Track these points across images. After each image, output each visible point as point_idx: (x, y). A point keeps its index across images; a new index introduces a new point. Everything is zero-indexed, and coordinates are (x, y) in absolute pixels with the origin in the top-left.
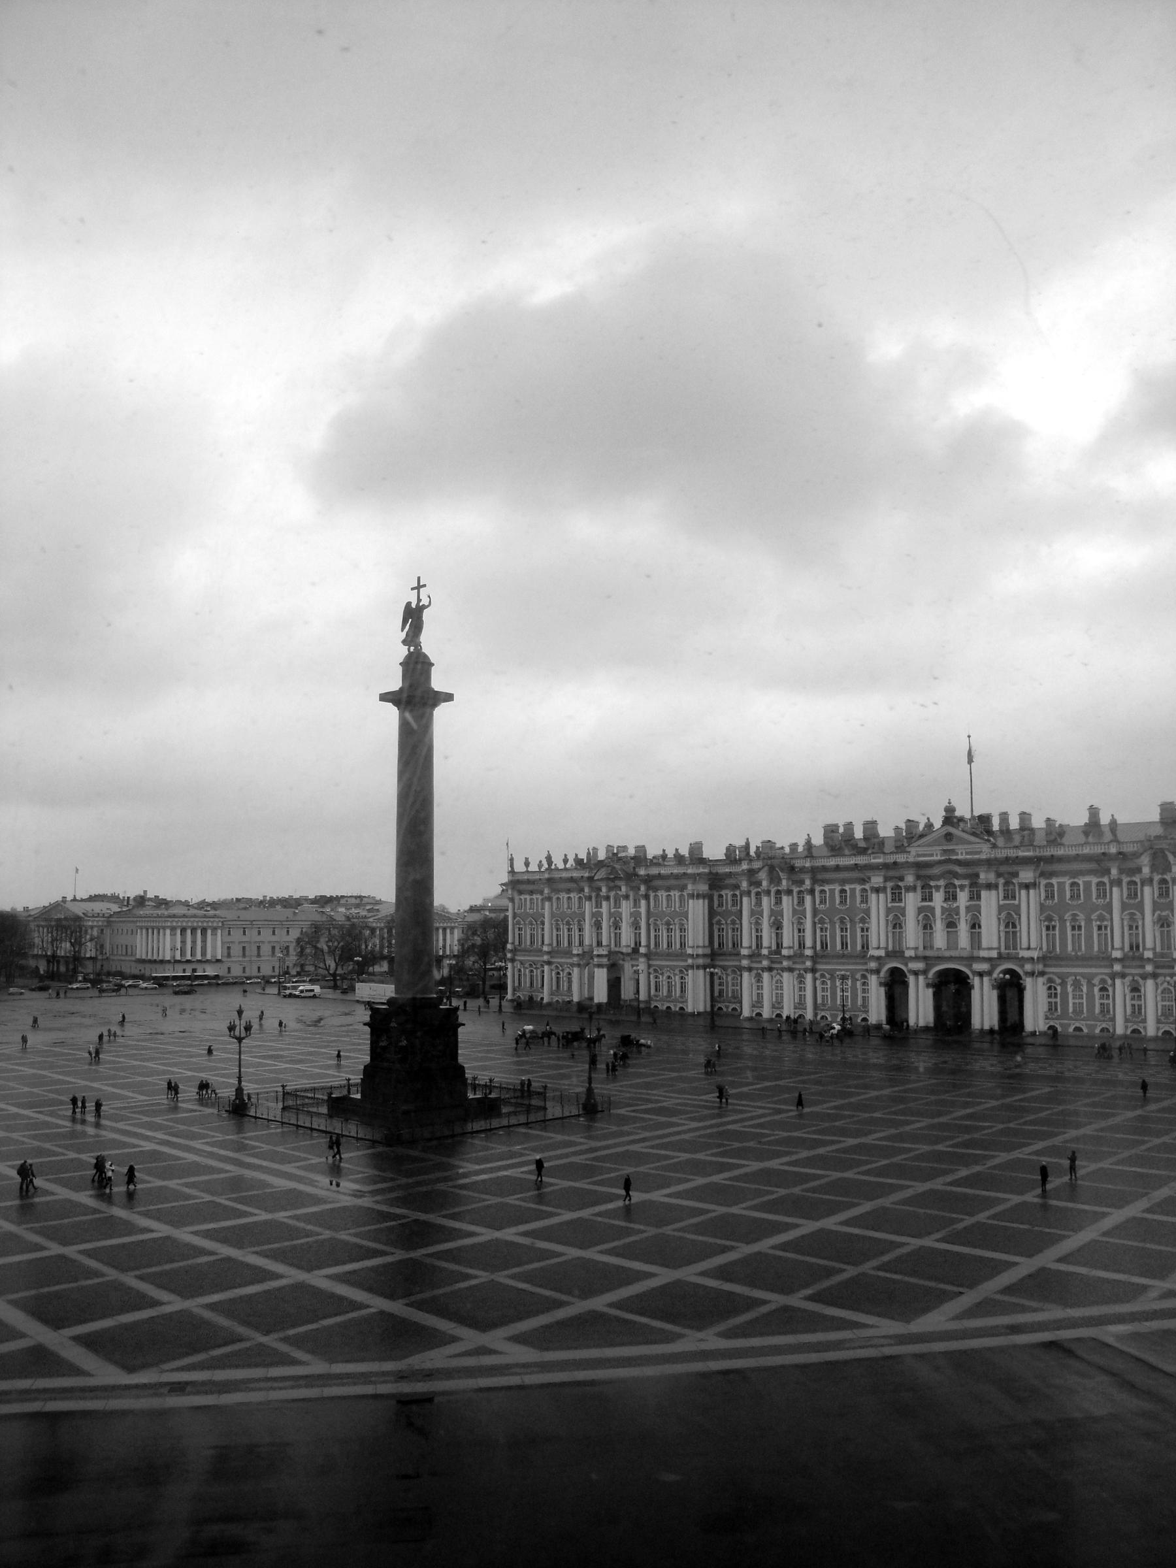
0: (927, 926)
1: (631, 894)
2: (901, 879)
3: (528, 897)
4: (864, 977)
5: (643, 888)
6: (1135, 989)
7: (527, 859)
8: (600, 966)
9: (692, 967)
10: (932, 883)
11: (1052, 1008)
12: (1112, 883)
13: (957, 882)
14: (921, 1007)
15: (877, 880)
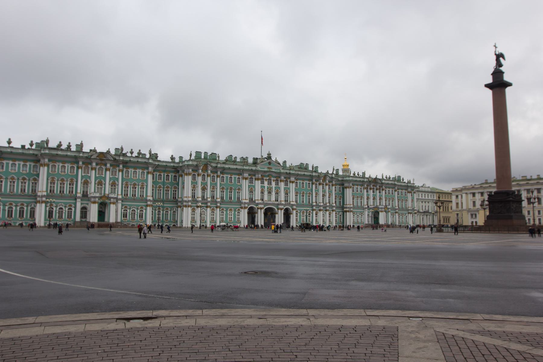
0: (262, 192)
1: (111, 168)
2: (255, 175)
3: (11, 162)
4: (239, 210)
5: (121, 166)
6: (316, 214)
7: (10, 139)
8: (114, 203)
9: (150, 206)
10: (265, 178)
11: (297, 220)
12: (313, 184)
13: (272, 179)
14: (260, 219)
15: (246, 175)
